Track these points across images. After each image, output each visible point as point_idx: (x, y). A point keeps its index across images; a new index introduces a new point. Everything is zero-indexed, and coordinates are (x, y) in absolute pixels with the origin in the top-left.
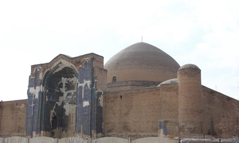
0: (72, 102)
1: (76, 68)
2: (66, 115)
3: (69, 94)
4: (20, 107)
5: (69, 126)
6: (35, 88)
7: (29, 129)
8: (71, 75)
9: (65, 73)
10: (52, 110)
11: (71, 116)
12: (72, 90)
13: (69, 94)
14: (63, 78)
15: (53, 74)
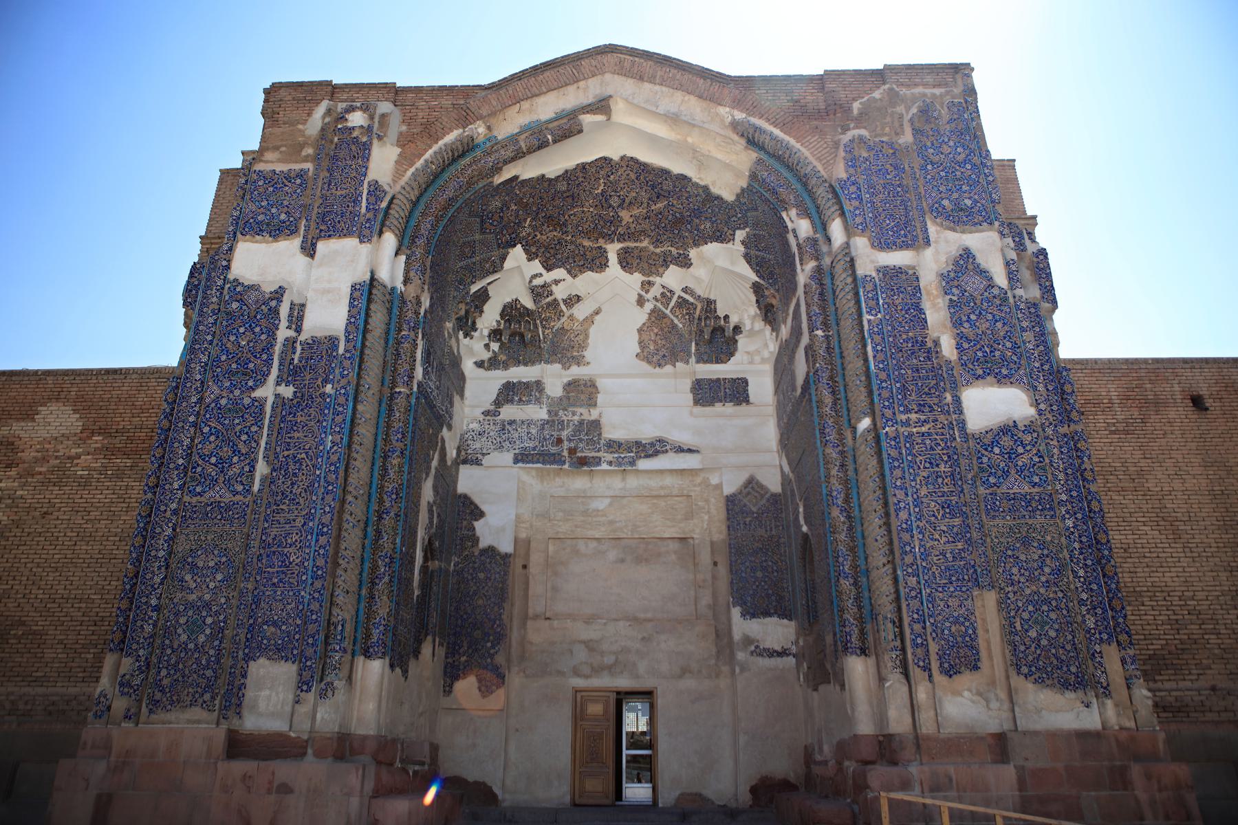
0: (554, 450)
1: (798, 146)
2: (491, 551)
3: (510, 393)
4: (18, 429)
5: (515, 636)
6: (309, 250)
7: (194, 627)
8: (586, 243)
9: (549, 219)
10: (427, 475)
11: (536, 559)
12: (547, 362)
13: (510, 393)
14: (517, 253)
15: (499, 180)
